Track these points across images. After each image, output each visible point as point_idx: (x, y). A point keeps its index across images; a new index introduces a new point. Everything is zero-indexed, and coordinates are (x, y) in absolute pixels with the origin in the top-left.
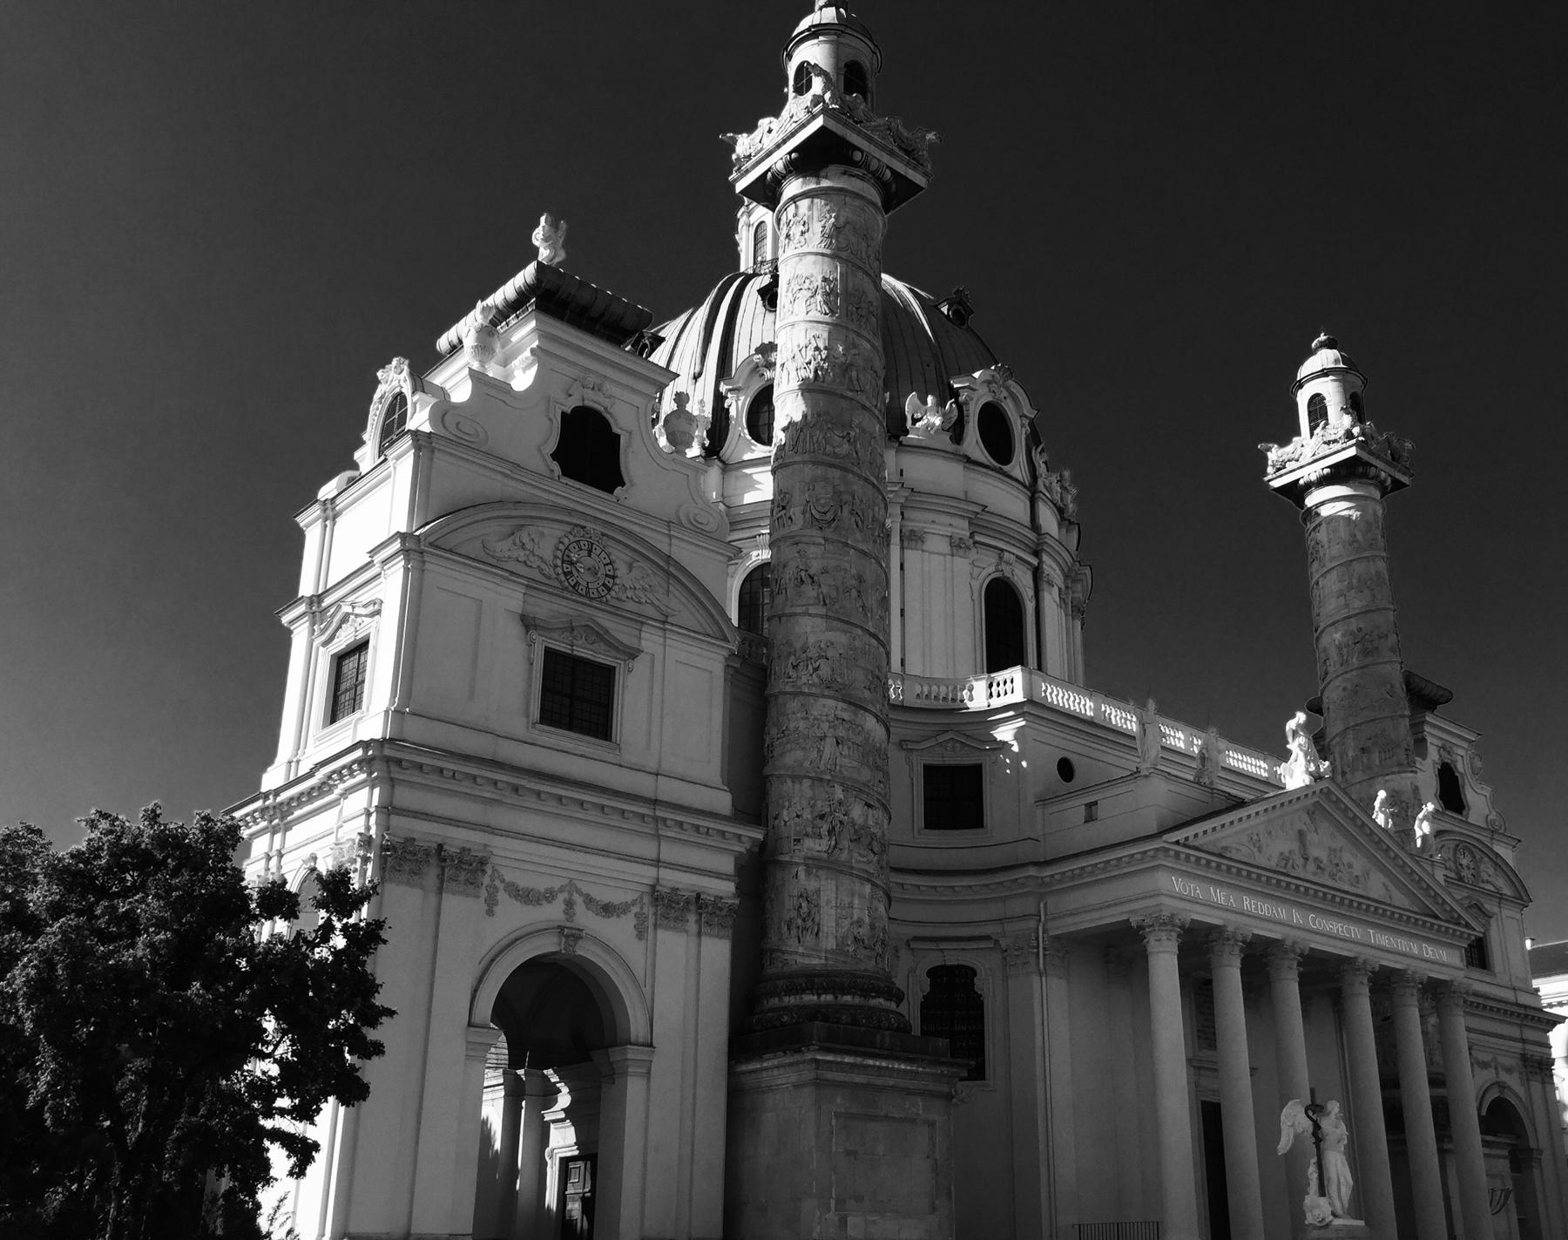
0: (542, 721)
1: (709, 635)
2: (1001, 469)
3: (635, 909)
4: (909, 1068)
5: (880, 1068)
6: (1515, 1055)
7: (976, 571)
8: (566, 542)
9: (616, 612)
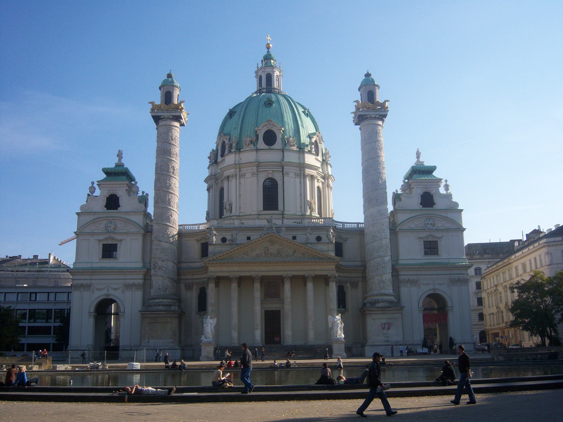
0: (102, 258)
1: (138, 232)
2: (270, 148)
3: (121, 288)
5: (158, 313)
6: (447, 279)
7: (260, 179)
9: (116, 233)
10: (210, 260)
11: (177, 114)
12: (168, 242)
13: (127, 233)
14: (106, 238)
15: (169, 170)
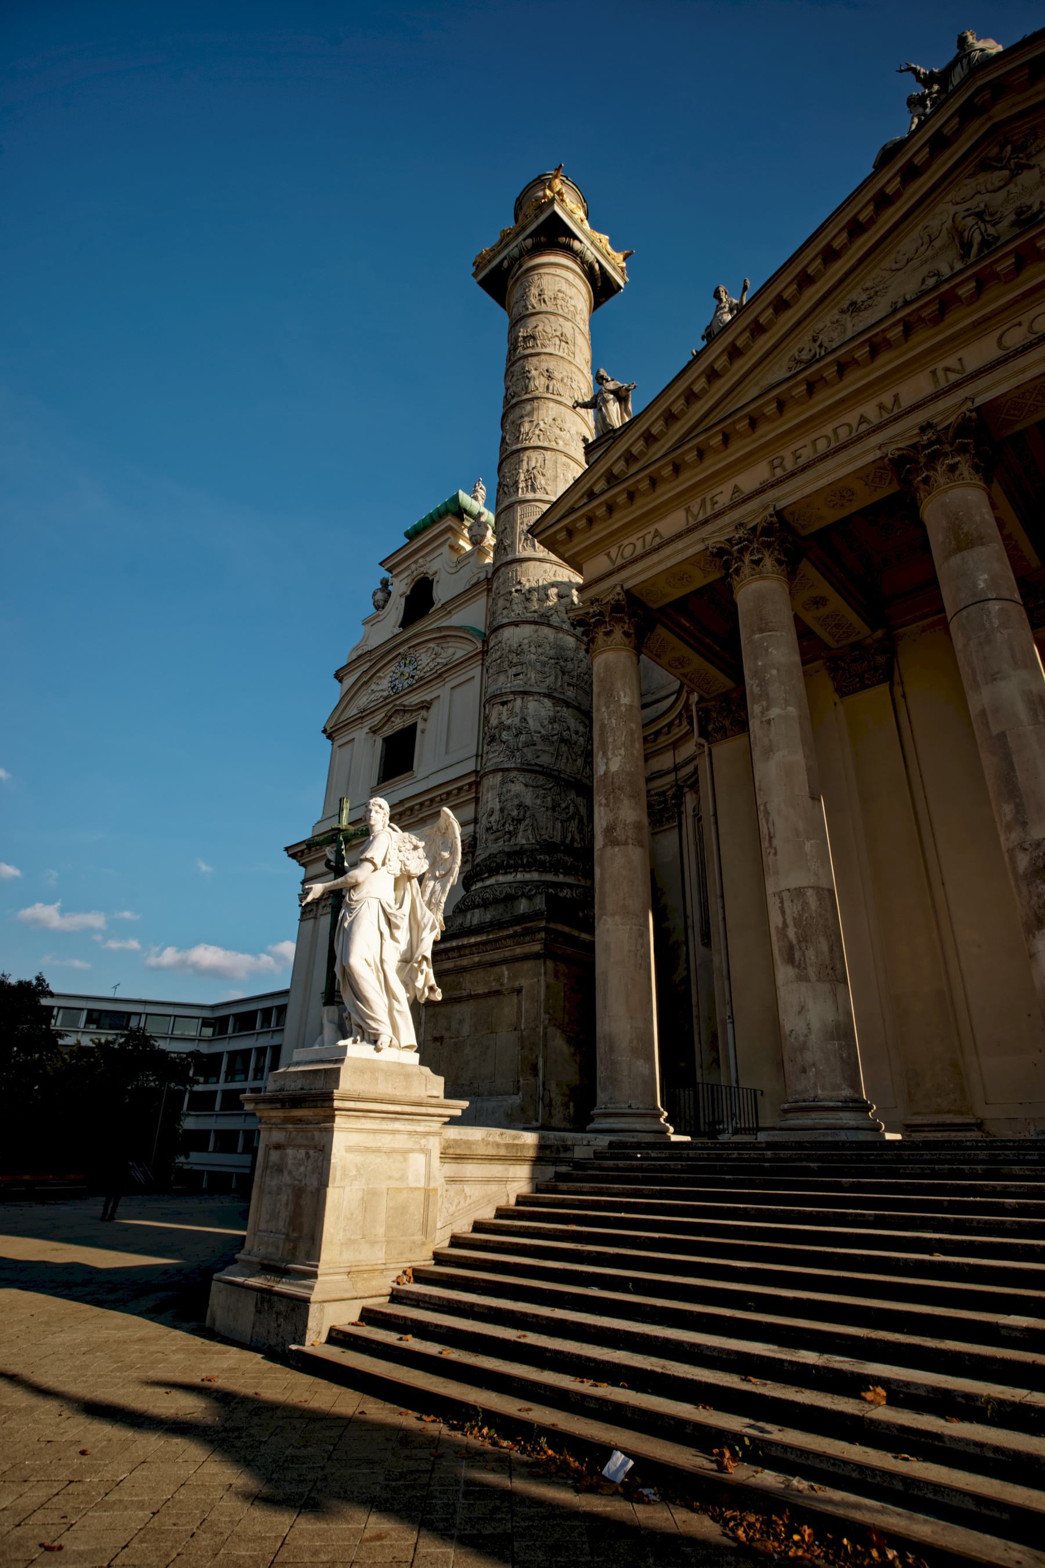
4: (479, 939)
5: (458, 948)
8: (393, 668)
10: (572, 510)
11: (542, 218)
12: (524, 622)
13: (440, 676)
14: (386, 715)
15: (527, 387)
